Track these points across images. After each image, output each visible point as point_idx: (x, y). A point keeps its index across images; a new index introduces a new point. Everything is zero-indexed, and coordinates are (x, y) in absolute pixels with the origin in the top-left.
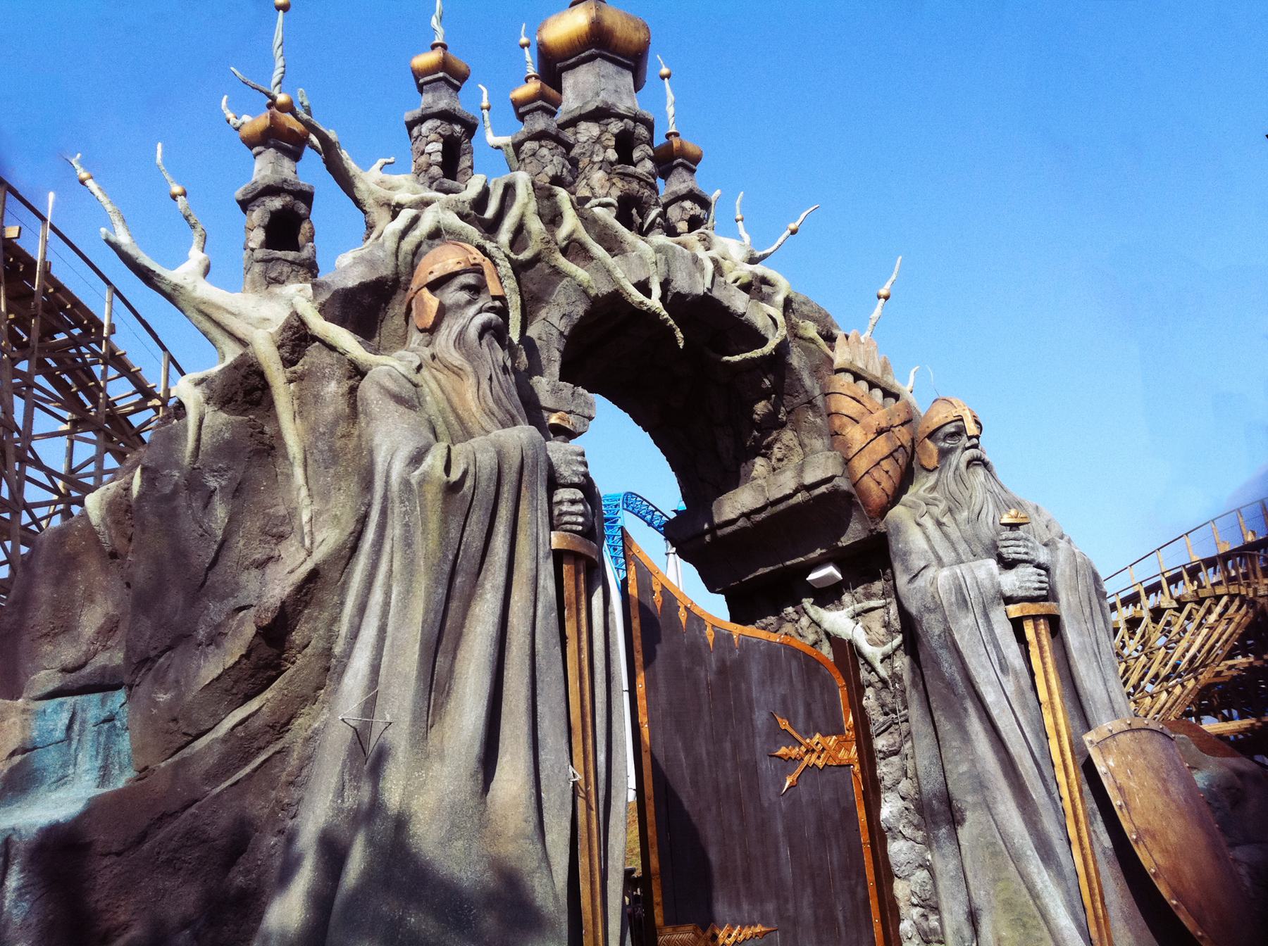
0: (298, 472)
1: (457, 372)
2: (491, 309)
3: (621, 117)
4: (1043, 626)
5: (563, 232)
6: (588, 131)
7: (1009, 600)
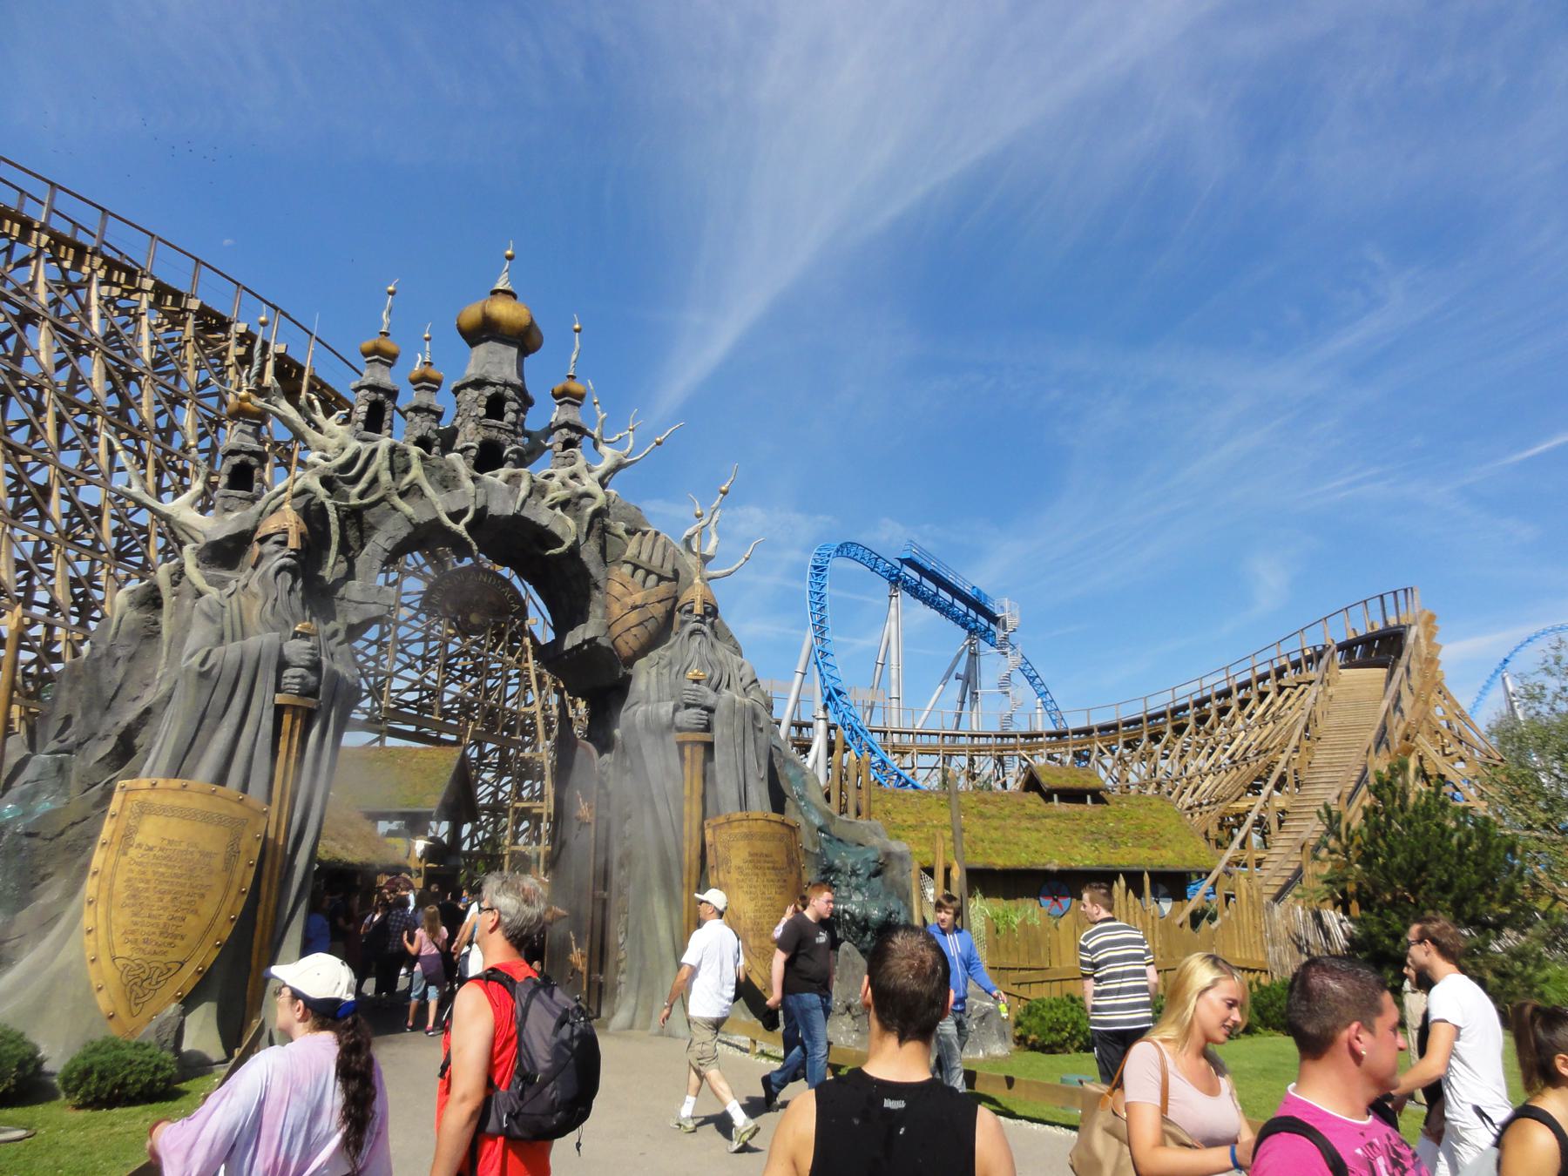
0: (165, 649)
1: (255, 596)
2: (289, 556)
3: (493, 384)
4: (700, 751)
5: (408, 479)
6: (471, 393)
7: (679, 730)
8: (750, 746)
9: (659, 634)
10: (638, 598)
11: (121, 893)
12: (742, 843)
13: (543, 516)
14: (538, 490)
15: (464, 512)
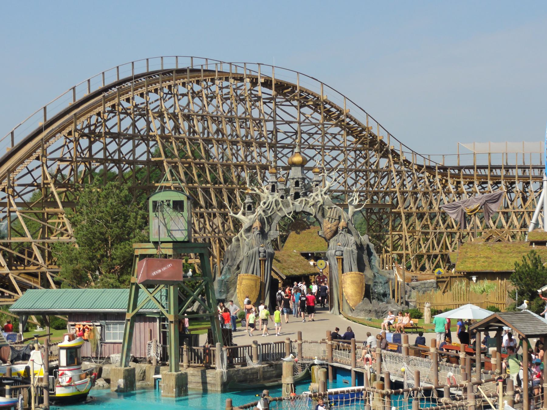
5: (279, 207)
8: (352, 258)
9: (336, 233)
10: (329, 226)
11: (242, 292)
12: (350, 279)
13: (308, 210)
15: (291, 213)
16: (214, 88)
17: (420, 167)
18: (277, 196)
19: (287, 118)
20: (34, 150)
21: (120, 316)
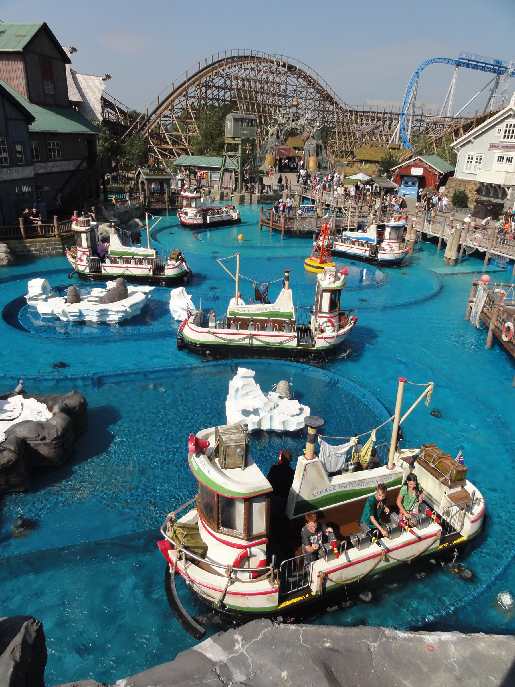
9: (308, 138)
13: (297, 127)
14: (297, 124)
16: (261, 66)
17: (347, 110)
18: (285, 120)
19: (292, 83)
20: (182, 92)
21: (218, 169)
